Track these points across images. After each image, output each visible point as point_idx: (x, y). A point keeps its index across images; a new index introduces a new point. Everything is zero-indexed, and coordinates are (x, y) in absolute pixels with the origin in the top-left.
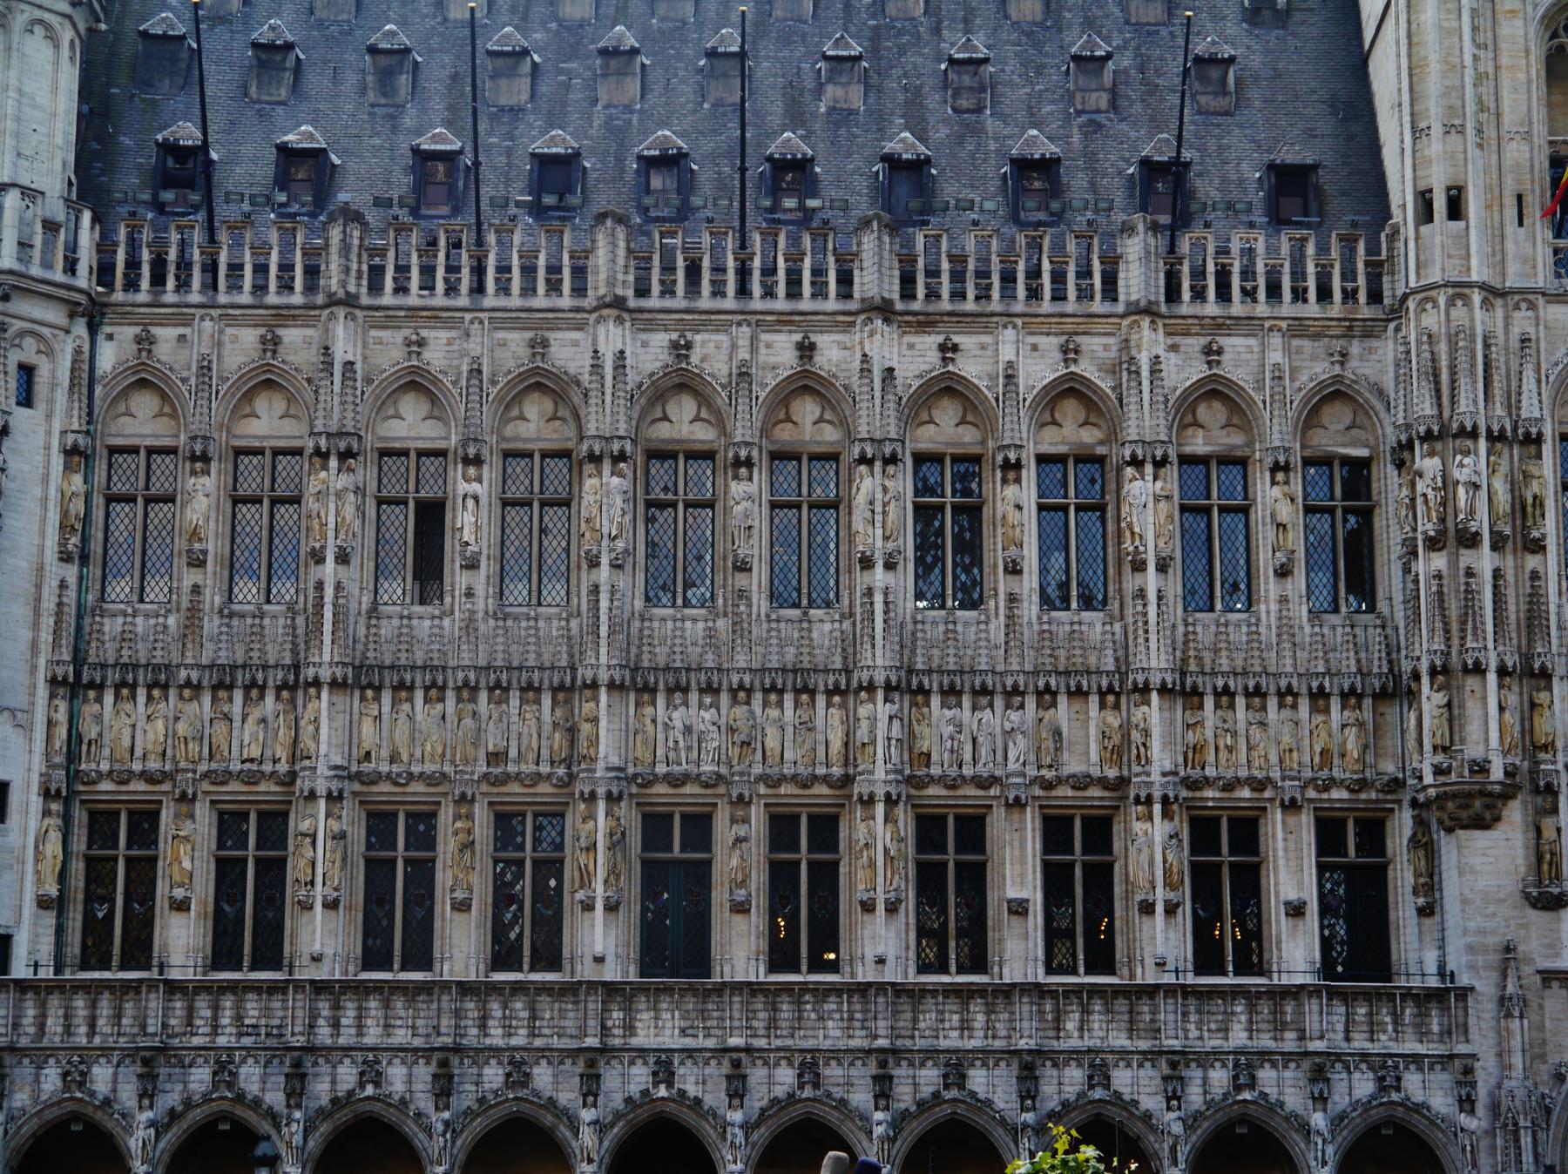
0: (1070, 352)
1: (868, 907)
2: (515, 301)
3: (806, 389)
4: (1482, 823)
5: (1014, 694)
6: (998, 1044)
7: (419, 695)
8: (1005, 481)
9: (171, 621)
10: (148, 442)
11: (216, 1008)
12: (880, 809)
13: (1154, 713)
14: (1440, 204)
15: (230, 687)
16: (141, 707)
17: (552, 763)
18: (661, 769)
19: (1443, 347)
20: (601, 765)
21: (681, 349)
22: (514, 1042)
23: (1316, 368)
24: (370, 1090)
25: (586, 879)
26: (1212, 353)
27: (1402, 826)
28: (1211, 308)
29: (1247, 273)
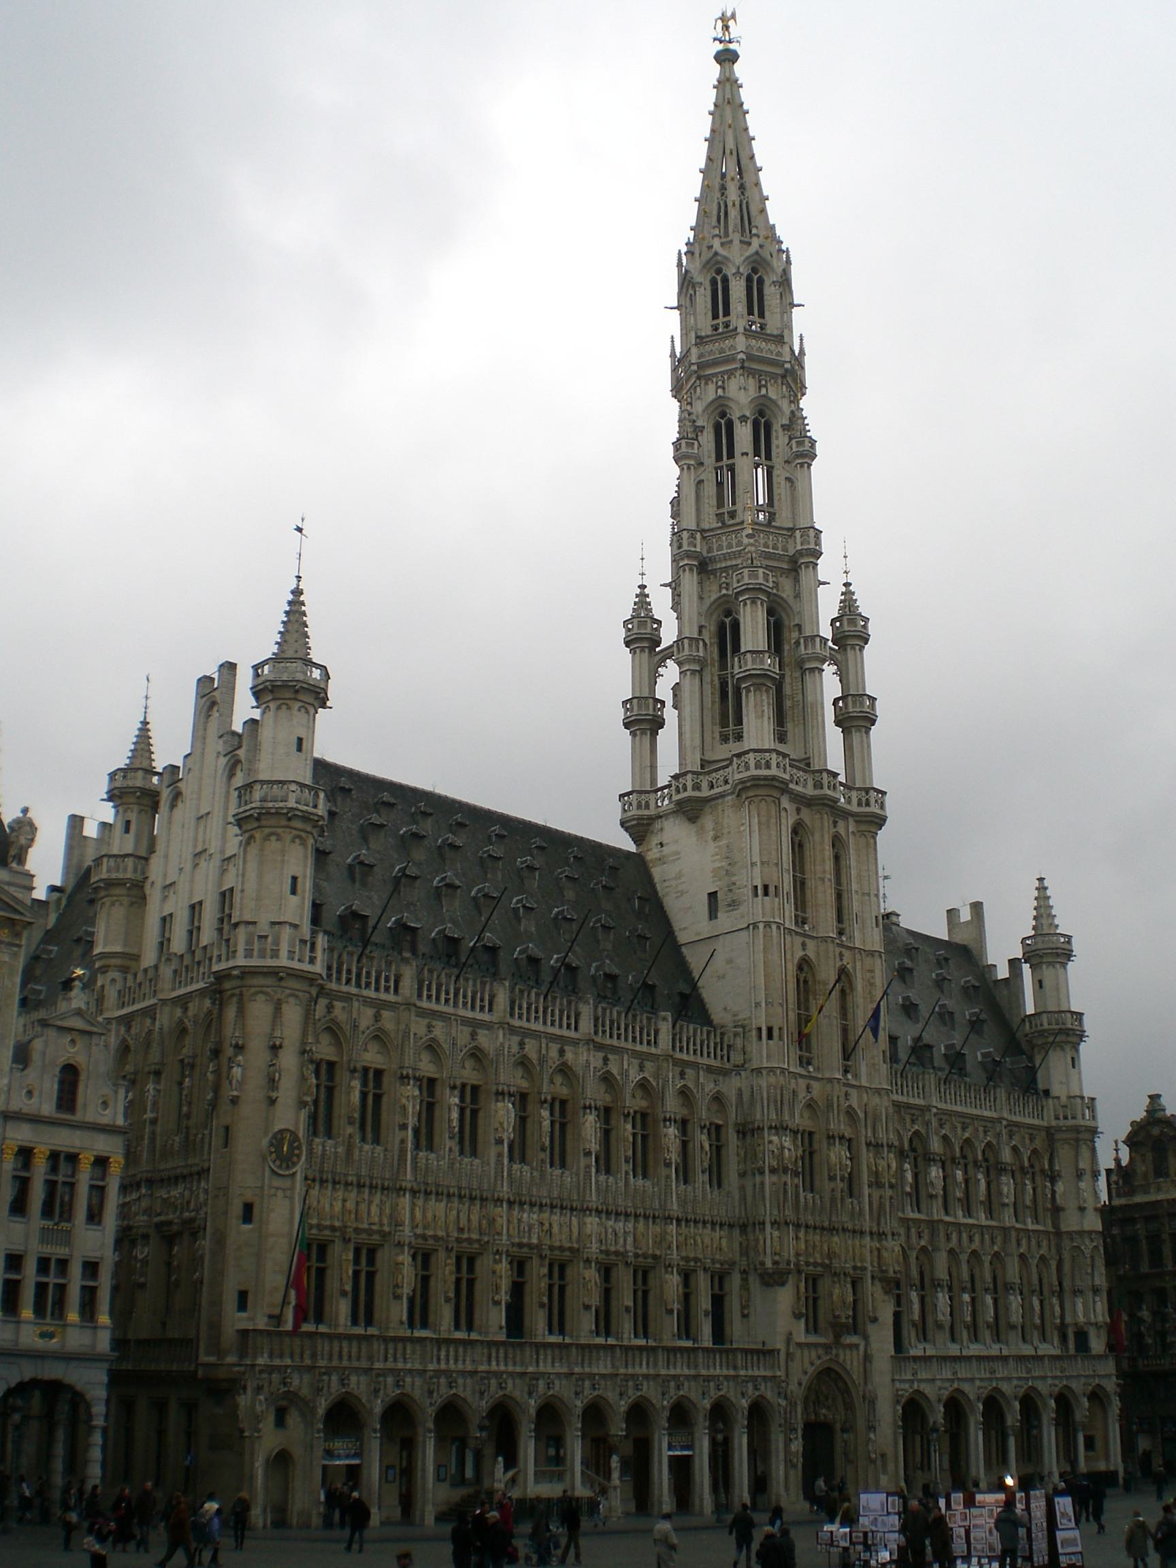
0: (641, 1068)
1: (587, 1307)
2: (470, 1014)
3: (561, 1071)
4: (783, 1284)
5: (627, 1215)
6: (652, 1371)
7: (433, 1197)
8: (625, 1122)
9: (340, 1150)
10: (328, 1058)
11: (396, 1349)
12: (593, 1264)
13: (672, 1228)
14: (776, 1033)
15: (364, 1186)
16: (329, 1194)
17: (481, 1234)
18: (517, 1240)
19: (779, 1092)
20: (505, 1237)
21: (521, 1045)
22: (502, 1368)
23: (710, 1087)
24: (454, 1391)
25: (497, 1289)
26: (682, 1074)
27: (735, 1280)
28: (685, 1057)
29: (694, 1044)
